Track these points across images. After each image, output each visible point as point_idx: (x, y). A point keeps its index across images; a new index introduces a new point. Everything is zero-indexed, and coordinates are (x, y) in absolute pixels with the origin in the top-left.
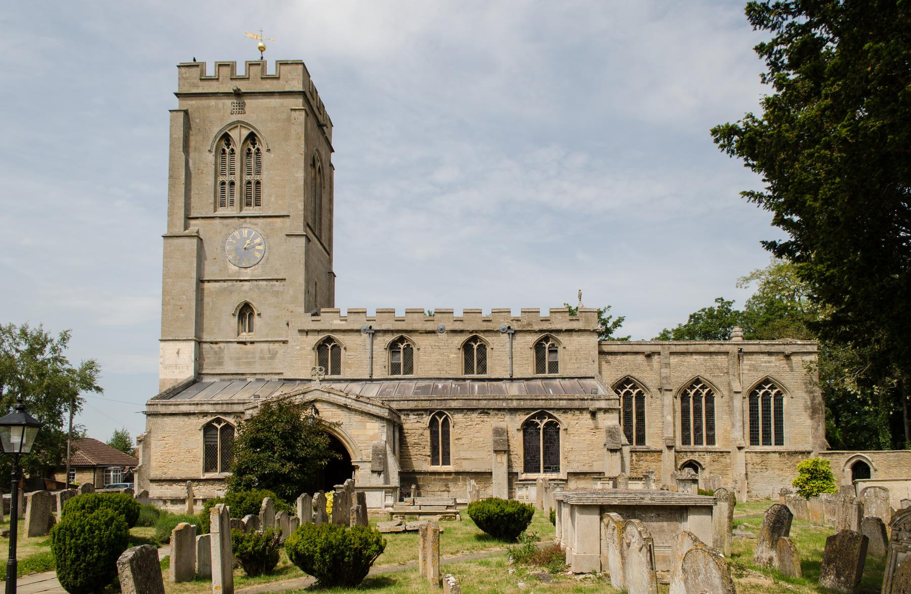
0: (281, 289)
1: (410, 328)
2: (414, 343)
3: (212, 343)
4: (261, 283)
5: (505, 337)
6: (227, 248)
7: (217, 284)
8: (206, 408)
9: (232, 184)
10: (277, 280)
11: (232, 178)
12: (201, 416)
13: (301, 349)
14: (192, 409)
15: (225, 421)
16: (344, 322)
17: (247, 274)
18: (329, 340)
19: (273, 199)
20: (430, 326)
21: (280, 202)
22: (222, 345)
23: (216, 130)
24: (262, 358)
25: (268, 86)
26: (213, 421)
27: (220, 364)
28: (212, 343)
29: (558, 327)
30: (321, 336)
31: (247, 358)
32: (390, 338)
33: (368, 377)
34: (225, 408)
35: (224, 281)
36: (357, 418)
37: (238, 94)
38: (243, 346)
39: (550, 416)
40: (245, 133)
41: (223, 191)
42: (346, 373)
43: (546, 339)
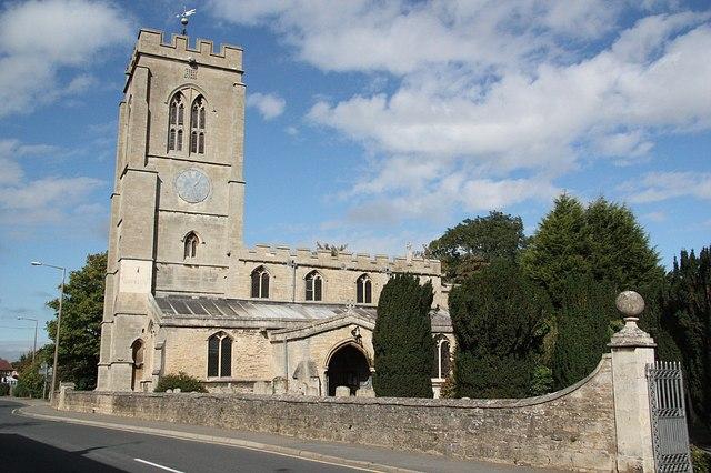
0: (222, 224)
7: (169, 214)
9: (180, 132)
11: (181, 127)
13: (241, 274)
17: (194, 208)
18: (261, 268)
19: (217, 150)
23: (172, 88)
34: (226, 324)
37: (193, 64)
39: (445, 338)
40: (196, 94)
41: (173, 137)
42: (273, 296)
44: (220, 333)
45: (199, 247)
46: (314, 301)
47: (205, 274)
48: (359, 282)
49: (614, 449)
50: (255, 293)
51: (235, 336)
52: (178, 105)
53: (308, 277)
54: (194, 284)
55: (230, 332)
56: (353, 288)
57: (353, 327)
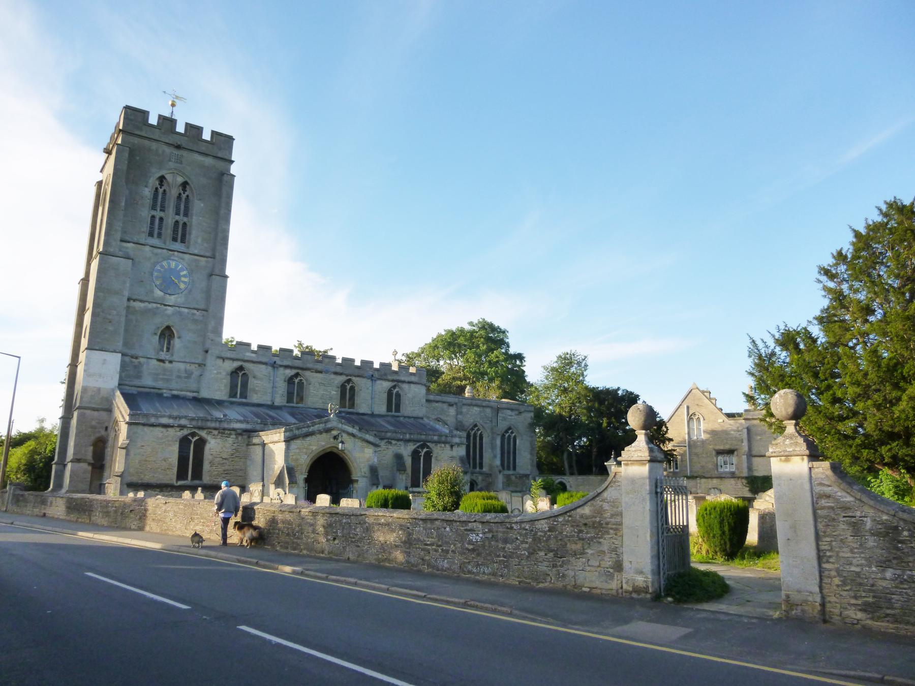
1: (305, 366)
2: (307, 380)
3: (132, 357)
4: (183, 310)
5: (369, 382)
6: (155, 274)
7: (142, 305)
8: (183, 422)
9: (161, 219)
10: (198, 310)
12: (178, 429)
13: (218, 373)
14: (171, 421)
15: (198, 435)
16: (253, 355)
18: (241, 368)
20: (319, 367)
21: (205, 245)
22: (141, 360)
24: (179, 377)
25: (203, 148)
26: (189, 435)
27: (139, 376)
28: (132, 357)
29: (403, 379)
30: (236, 364)
31: (164, 375)
32: (290, 373)
33: (269, 403)
34: (200, 424)
35: (150, 302)
36: (359, 443)
38: (162, 364)
39: (428, 447)
40: (180, 180)
43: (394, 387)
44: (193, 434)
45: (177, 343)
46: (294, 405)
47: (179, 371)
48: (343, 387)
49: (618, 567)
50: (233, 394)
51: (209, 438)
52: (161, 191)
53: (290, 381)
54: (167, 380)
55: (203, 434)
56: (335, 393)
57: (335, 433)
